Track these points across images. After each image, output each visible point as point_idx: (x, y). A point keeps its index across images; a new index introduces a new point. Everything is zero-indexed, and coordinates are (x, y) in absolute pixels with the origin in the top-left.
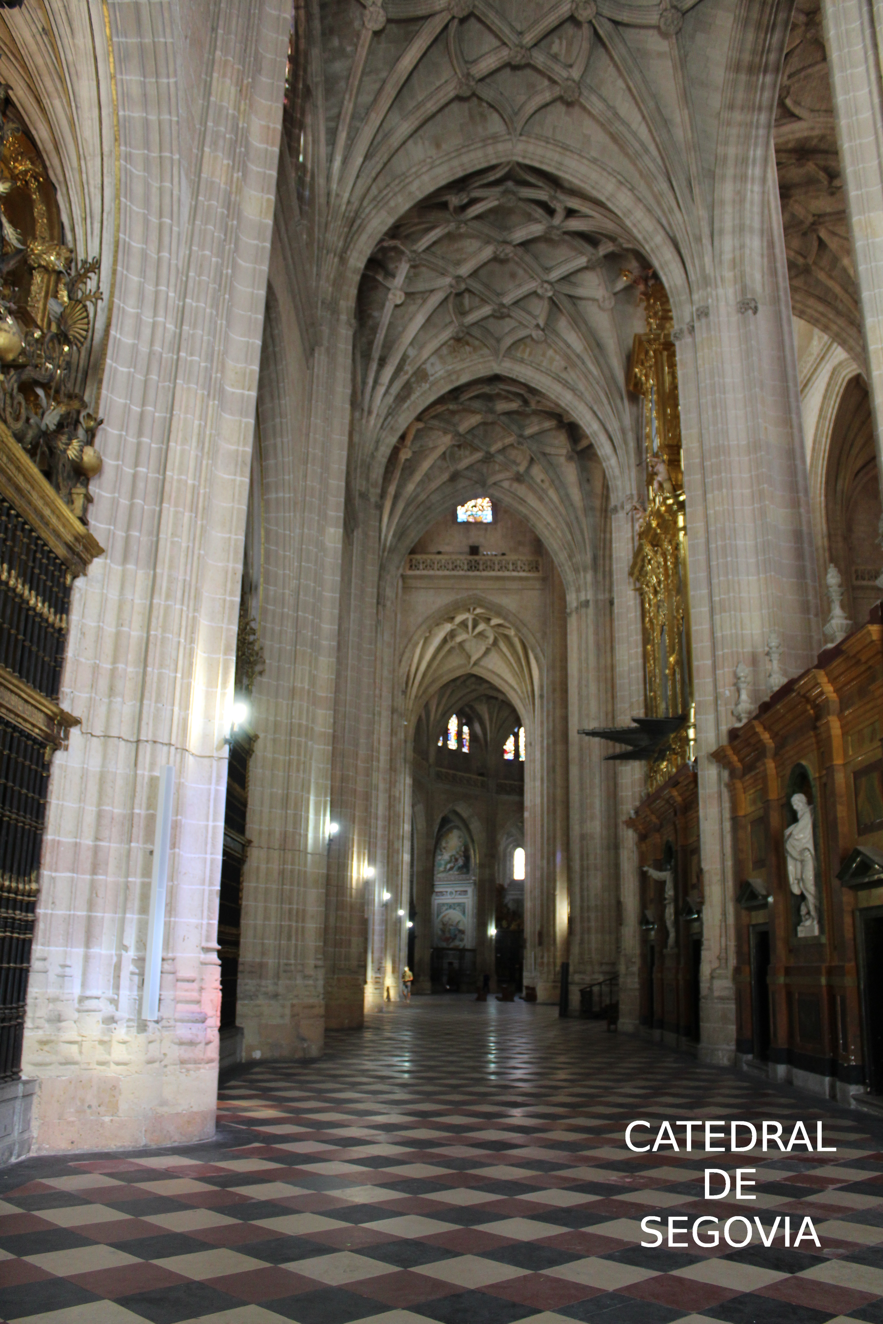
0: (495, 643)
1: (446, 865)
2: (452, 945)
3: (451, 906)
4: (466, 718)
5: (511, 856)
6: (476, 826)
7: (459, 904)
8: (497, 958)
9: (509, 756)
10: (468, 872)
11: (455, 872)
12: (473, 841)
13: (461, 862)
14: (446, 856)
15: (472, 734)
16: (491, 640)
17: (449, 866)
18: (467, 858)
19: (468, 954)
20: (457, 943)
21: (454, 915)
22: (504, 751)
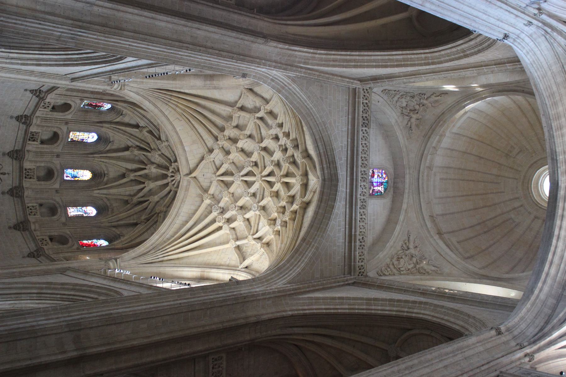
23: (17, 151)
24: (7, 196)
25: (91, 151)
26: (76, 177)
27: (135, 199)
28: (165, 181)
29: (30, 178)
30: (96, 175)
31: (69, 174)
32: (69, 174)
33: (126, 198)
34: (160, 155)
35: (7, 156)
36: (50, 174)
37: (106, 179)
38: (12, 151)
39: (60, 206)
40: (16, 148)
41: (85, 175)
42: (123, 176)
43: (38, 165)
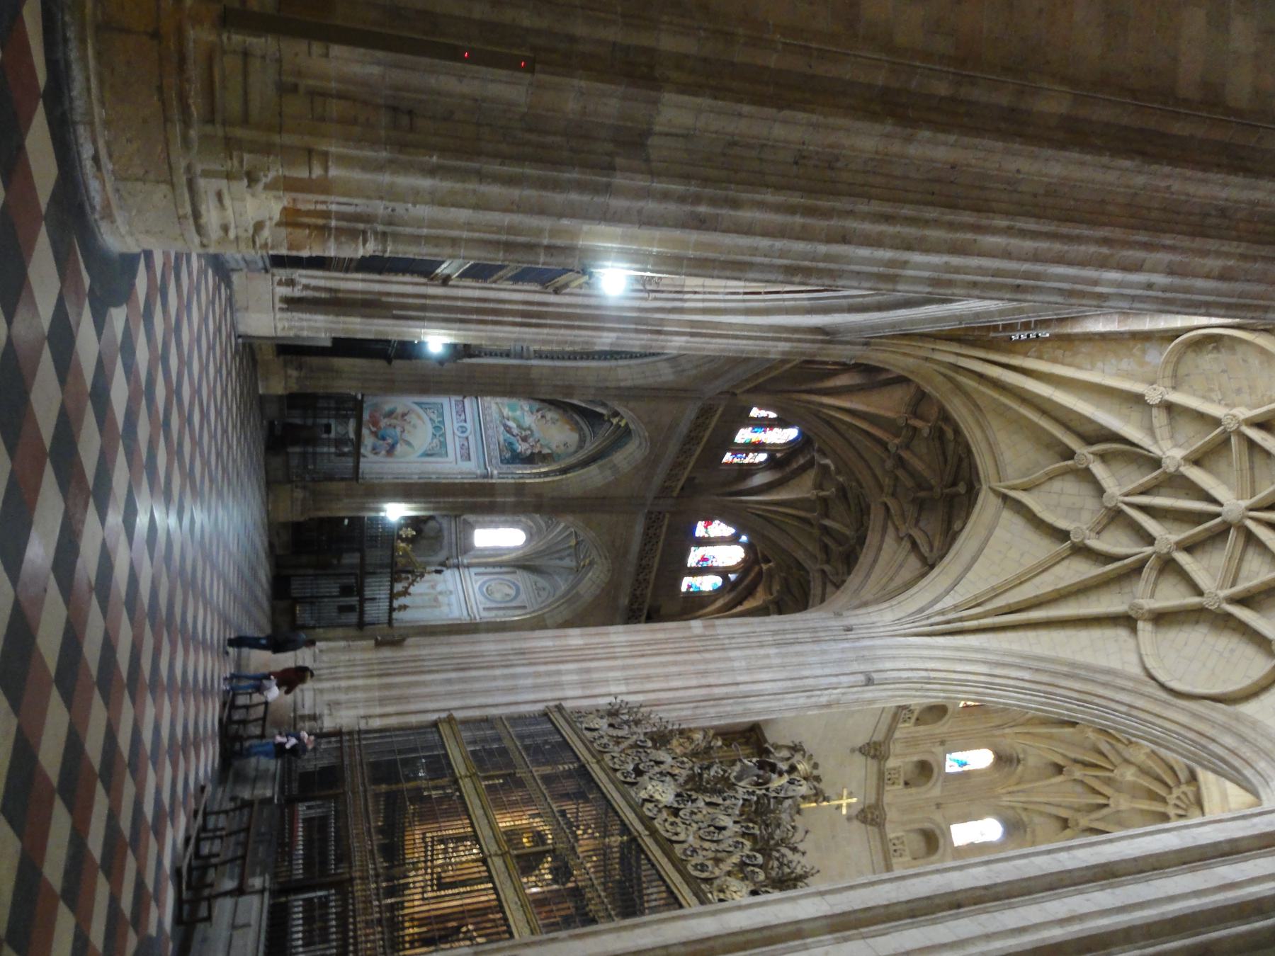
0: (1082, 551)
1: (515, 420)
2: (365, 432)
3: (438, 428)
4: (780, 459)
5: (513, 524)
6: (594, 477)
7: (443, 444)
8: (342, 519)
9: (700, 530)
10: (504, 461)
11: (502, 436)
12: (564, 471)
13: (521, 447)
14: (529, 420)
15: (751, 469)
16: (1094, 543)
17: (511, 424)
18: (530, 459)
19: (350, 462)
20: (368, 440)
21: (420, 434)
22: (709, 521)
23: (875, 743)
24: (856, 824)
25: (998, 722)
26: (965, 764)
27: (1084, 822)
28: (1158, 807)
29: (893, 784)
30: (1003, 760)
31: (953, 763)
32: (953, 763)
33: (1064, 813)
34: (1148, 756)
35: (857, 753)
36: (925, 770)
37: (1020, 768)
38: (868, 744)
39: (942, 830)
40: (875, 739)
41: (980, 759)
42: (1059, 769)
43: (907, 759)
